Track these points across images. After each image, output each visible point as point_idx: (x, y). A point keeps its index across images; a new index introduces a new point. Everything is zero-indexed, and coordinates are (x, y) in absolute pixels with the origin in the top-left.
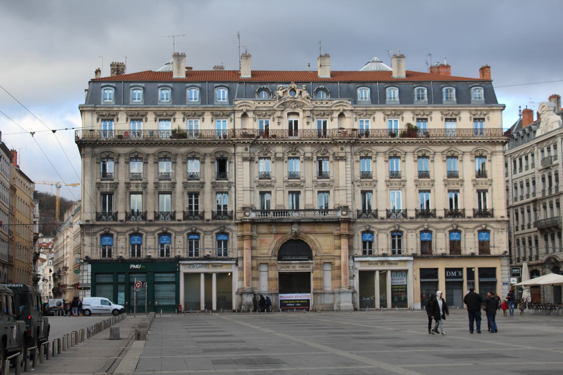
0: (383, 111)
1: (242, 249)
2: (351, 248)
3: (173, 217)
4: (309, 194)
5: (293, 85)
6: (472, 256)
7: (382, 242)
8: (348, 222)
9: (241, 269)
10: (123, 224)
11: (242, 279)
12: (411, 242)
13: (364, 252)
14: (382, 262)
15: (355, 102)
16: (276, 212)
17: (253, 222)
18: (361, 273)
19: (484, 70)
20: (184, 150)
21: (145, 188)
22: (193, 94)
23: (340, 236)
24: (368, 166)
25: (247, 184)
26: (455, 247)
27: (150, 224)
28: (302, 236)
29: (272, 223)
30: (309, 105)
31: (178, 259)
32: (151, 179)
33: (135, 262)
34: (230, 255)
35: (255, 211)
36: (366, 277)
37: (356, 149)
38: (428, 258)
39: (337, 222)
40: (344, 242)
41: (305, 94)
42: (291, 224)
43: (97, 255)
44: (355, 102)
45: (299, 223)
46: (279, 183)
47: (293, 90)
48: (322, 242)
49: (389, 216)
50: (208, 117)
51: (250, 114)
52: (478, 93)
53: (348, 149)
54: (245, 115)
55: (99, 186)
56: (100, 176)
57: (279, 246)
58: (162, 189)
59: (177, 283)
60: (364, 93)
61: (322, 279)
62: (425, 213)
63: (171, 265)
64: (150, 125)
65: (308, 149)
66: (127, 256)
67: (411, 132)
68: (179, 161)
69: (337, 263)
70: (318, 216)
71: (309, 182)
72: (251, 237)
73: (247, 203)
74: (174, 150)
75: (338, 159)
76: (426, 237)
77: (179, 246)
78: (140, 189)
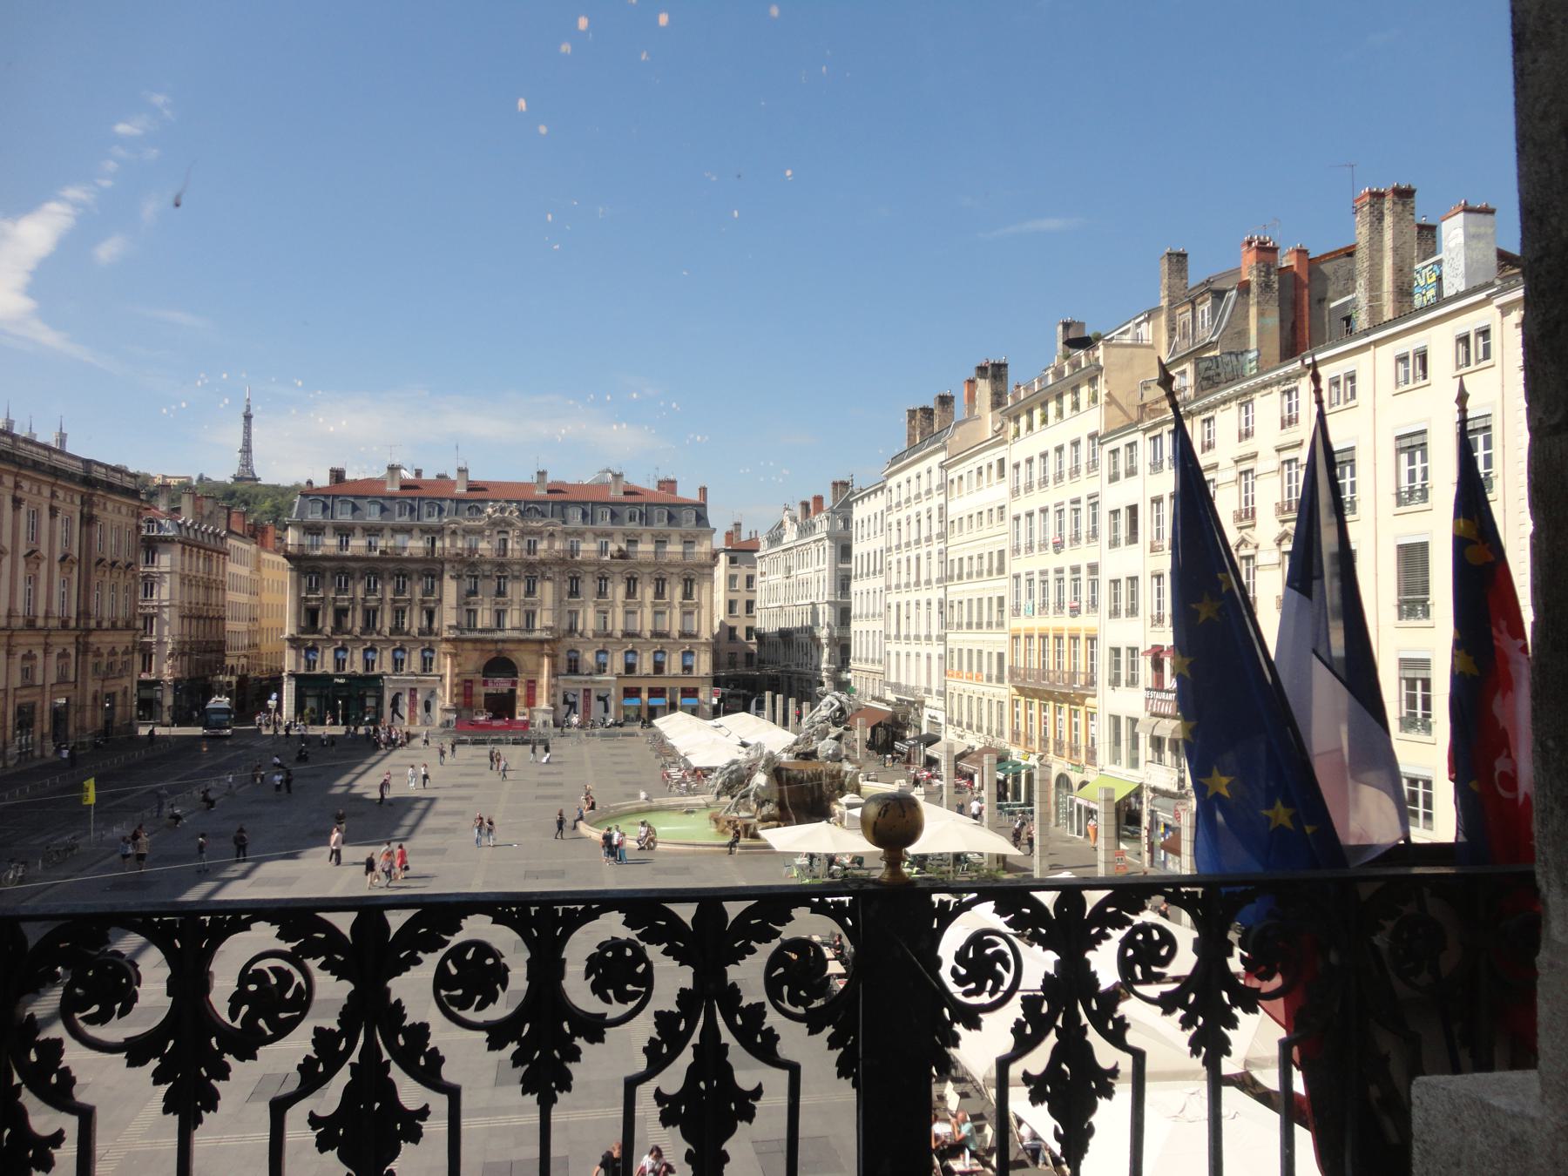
16: (482, 631)
19: (703, 490)
20: (391, 566)
28: (506, 655)
33: (339, 677)
34: (435, 671)
42: (496, 642)
45: (503, 641)
47: (502, 510)
51: (460, 532)
57: (484, 662)
66: (331, 670)
77: (383, 664)
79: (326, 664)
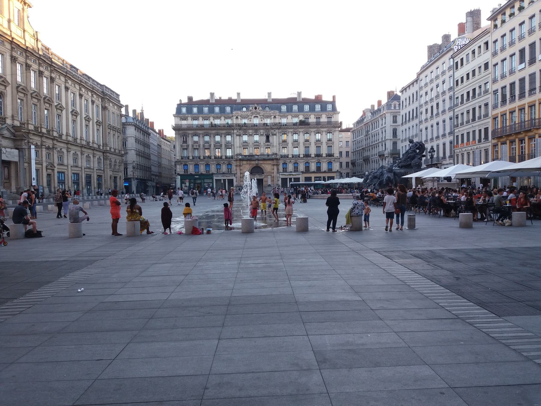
0: (291, 115)
1: (236, 170)
2: (278, 169)
3: (211, 158)
4: (262, 149)
5: (256, 105)
6: (325, 172)
7: (290, 167)
8: (277, 159)
9: (236, 178)
10: (191, 161)
11: (237, 181)
12: (302, 167)
13: (284, 171)
14: (290, 175)
15: (280, 112)
17: (240, 160)
18: (282, 179)
20: (214, 132)
21: (199, 146)
22: (217, 109)
23: (274, 165)
24: (284, 137)
25: (238, 145)
26: (319, 169)
27: (202, 160)
29: (247, 160)
30: (262, 113)
31: (213, 174)
32: (201, 143)
35: (242, 155)
36: (284, 181)
37: (280, 131)
38: (308, 173)
39: (272, 160)
40: (275, 167)
41: (260, 108)
43: (182, 173)
44: (280, 112)
46: (251, 144)
47: (256, 108)
48: (267, 167)
49: (293, 157)
50: (223, 118)
51: (239, 117)
52: (329, 107)
53: (277, 131)
54: (237, 118)
55: (181, 146)
56: (182, 142)
58: (206, 147)
59: (213, 183)
60: (284, 108)
61: (267, 181)
62: (307, 156)
63: (210, 176)
64: (200, 122)
65: (262, 131)
66: (193, 173)
67: (302, 123)
68: (212, 136)
69: (273, 175)
70: (266, 157)
71: (262, 144)
72: (240, 166)
73: (238, 152)
74: (210, 132)
75: (273, 135)
76: (307, 165)
78: (198, 147)
79: (191, 169)
